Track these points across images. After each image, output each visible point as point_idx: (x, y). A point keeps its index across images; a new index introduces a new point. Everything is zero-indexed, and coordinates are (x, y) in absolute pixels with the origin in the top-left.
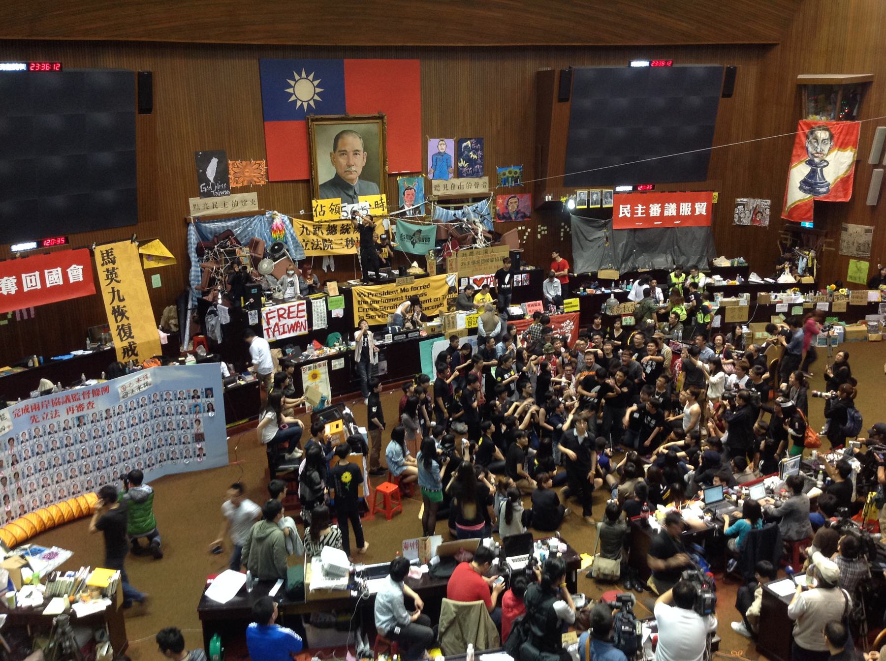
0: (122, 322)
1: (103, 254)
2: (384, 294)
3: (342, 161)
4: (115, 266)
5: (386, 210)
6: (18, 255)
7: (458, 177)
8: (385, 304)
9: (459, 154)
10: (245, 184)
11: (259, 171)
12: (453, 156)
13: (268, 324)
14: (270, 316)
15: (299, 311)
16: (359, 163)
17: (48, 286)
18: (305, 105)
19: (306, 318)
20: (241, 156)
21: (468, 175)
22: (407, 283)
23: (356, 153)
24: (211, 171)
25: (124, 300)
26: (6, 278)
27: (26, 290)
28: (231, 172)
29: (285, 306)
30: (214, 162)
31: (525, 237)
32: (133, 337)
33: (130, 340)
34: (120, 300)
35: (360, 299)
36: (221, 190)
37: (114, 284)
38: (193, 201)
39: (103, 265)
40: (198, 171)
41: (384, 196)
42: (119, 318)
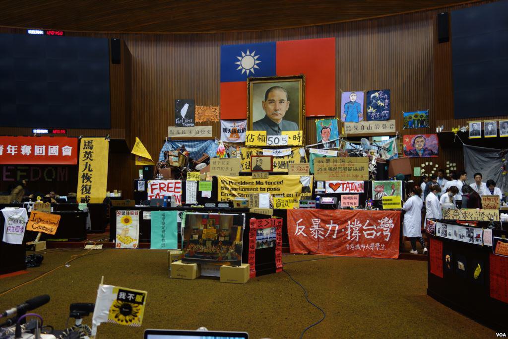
0: (87, 183)
1: (85, 143)
2: (242, 183)
3: (271, 107)
4: (92, 151)
5: (301, 142)
6: (35, 134)
7: (368, 121)
8: (242, 192)
9: (368, 102)
10: (205, 120)
11: (214, 113)
12: (362, 104)
13: (152, 193)
14: (154, 187)
15: (175, 188)
16: (283, 108)
17: (49, 155)
18: (248, 71)
19: (181, 194)
20: (205, 104)
21: (376, 119)
22: (262, 178)
23: (281, 101)
24: (184, 111)
25: (92, 171)
26: (25, 146)
27: (36, 154)
28: (197, 112)
29: (166, 182)
30: (186, 106)
31: (433, 172)
32: (90, 193)
33: (87, 194)
34: (89, 170)
35: (223, 185)
36: (189, 123)
37: (88, 161)
38: (170, 128)
39: (84, 149)
40: (176, 111)
41: (301, 132)
42: (85, 181)
